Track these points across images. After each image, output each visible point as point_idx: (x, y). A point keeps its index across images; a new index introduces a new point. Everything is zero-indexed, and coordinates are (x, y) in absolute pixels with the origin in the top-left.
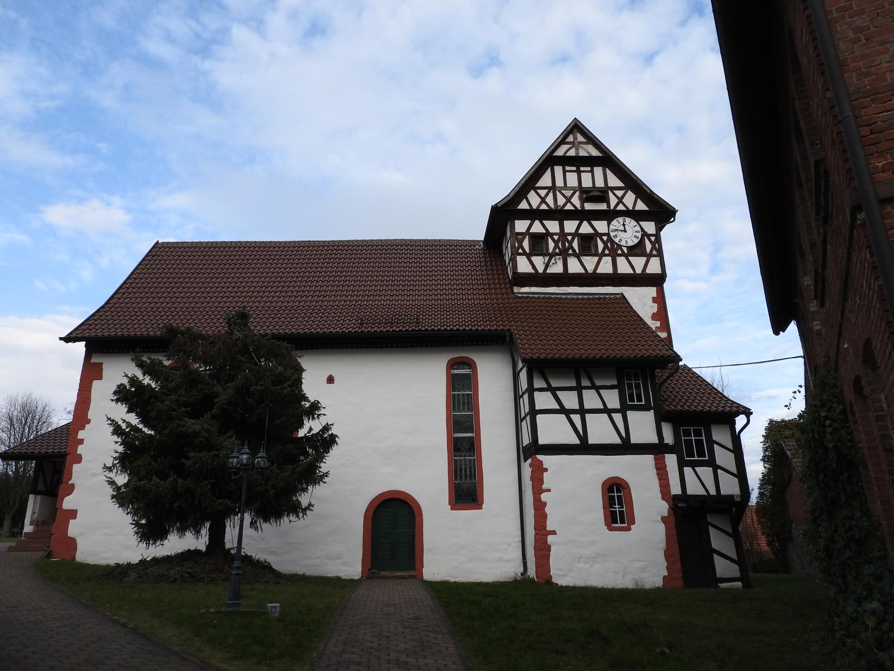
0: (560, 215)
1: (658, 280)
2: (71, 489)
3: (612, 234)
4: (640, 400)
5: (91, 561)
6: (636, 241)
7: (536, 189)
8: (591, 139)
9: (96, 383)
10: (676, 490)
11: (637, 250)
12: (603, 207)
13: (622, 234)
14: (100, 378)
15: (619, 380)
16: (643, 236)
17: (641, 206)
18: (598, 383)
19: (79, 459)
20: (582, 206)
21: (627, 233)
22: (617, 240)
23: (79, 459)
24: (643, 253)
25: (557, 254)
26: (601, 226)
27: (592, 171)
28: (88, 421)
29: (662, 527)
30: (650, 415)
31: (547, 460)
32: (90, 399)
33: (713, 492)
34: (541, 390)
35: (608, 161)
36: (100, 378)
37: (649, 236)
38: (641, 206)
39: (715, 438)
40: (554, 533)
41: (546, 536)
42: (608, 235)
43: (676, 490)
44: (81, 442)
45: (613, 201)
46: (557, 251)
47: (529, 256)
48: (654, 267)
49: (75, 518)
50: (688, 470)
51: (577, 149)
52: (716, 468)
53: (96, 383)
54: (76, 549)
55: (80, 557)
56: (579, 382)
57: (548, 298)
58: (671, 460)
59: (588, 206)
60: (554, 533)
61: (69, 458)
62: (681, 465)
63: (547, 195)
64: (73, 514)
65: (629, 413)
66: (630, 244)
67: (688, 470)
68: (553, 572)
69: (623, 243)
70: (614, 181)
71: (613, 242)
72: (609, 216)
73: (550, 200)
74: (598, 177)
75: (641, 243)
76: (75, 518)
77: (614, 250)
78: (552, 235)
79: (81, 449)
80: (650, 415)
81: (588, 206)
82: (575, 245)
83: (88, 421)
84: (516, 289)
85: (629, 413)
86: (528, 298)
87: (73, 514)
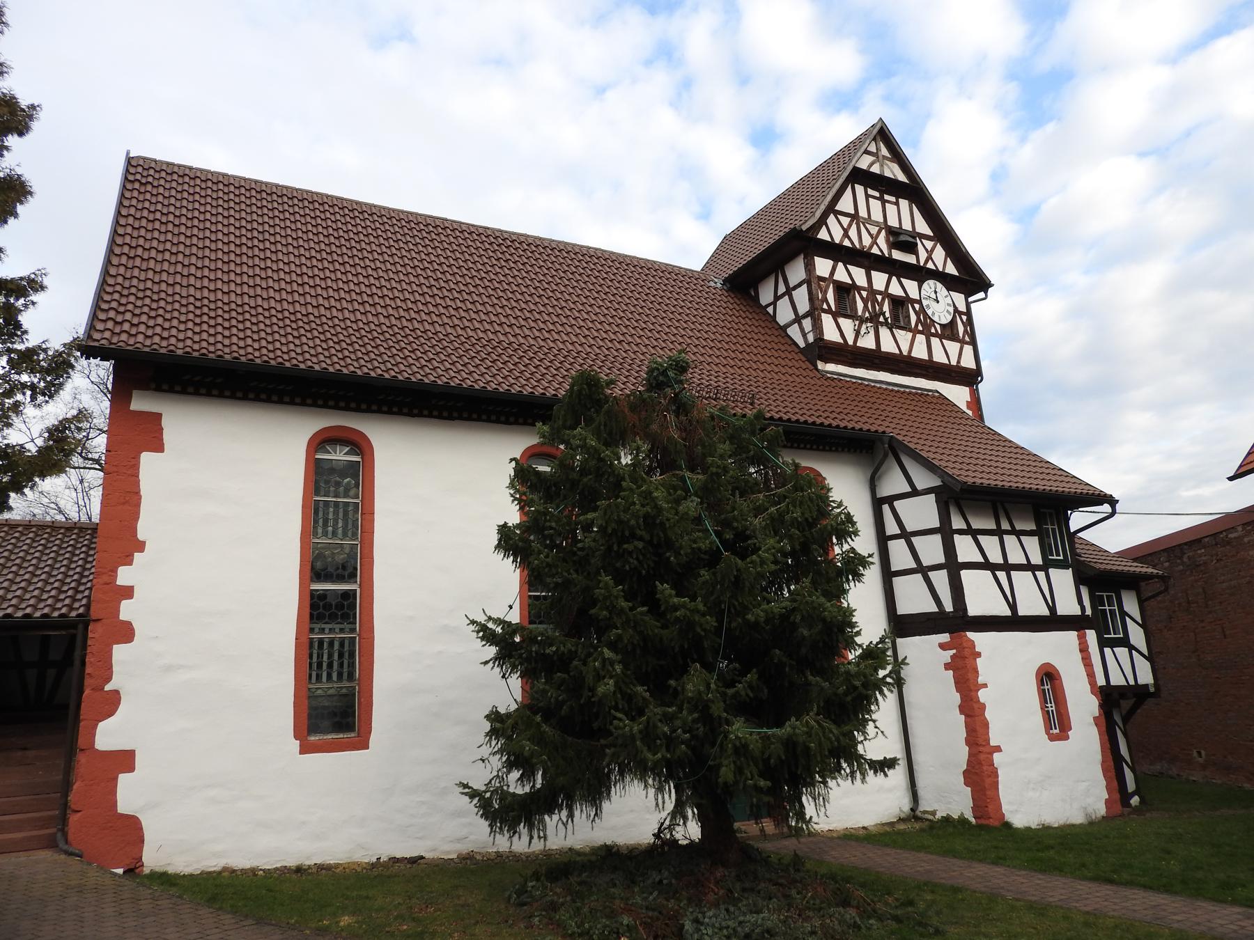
0: (869, 261)
1: (970, 378)
2: (111, 703)
3: (925, 303)
4: (1058, 555)
5: (184, 863)
6: (949, 318)
7: (838, 213)
8: (898, 156)
9: (148, 460)
10: (1101, 681)
11: (949, 332)
12: (911, 259)
13: (934, 304)
14: (159, 447)
15: (1039, 521)
16: (954, 316)
17: (951, 269)
18: (1019, 527)
19: (126, 633)
20: (890, 254)
21: (941, 304)
22: (929, 312)
23: (126, 633)
24: (954, 337)
25: (867, 320)
26: (911, 286)
27: (897, 204)
28: (141, 546)
29: (1095, 730)
30: (1069, 573)
31: (980, 639)
32: (137, 493)
33: (1132, 682)
34: (961, 532)
35: (915, 192)
36: (159, 447)
37: (961, 313)
38: (951, 269)
39: (1126, 609)
40: (998, 749)
41: (991, 754)
42: (920, 302)
43: (1101, 681)
44: (128, 592)
45: (923, 255)
46: (867, 315)
47: (835, 316)
48: (968, 362)
49: (131, 769)
50: (1107, 651)
51: (882, 166)
52: (1131, 648)
53: (148, 460)
54: (141, 840)
55: (153, 858)
56: (998, 524)
57: (861, 384)
58: (1091, 635)
59: (897, 255)
60: (998, 749)
61: (95, 632)
62: (1103, 643)
63: (850, 225)
64: (125, 760)
65: (1051, 571)
66: (944, 321)
67: (1107, 651)
68: (1005, 808)
69: (936, 319)
70: (923, 227)
71: (926, 314)
72: (920, 274)
73: (853, 233)
74: (903, 215)
75: (953, 323)
76: (131, 769)
77: (926, 327)
78: (859, 289)
79: (127, 610)
80: (1069, 573)
81: (897, 255)
82: (886, 308)
83: (141, 546)
84: (820, 365)
85: (1051, 571)
86: (838, 379)
87: (125, 760)
